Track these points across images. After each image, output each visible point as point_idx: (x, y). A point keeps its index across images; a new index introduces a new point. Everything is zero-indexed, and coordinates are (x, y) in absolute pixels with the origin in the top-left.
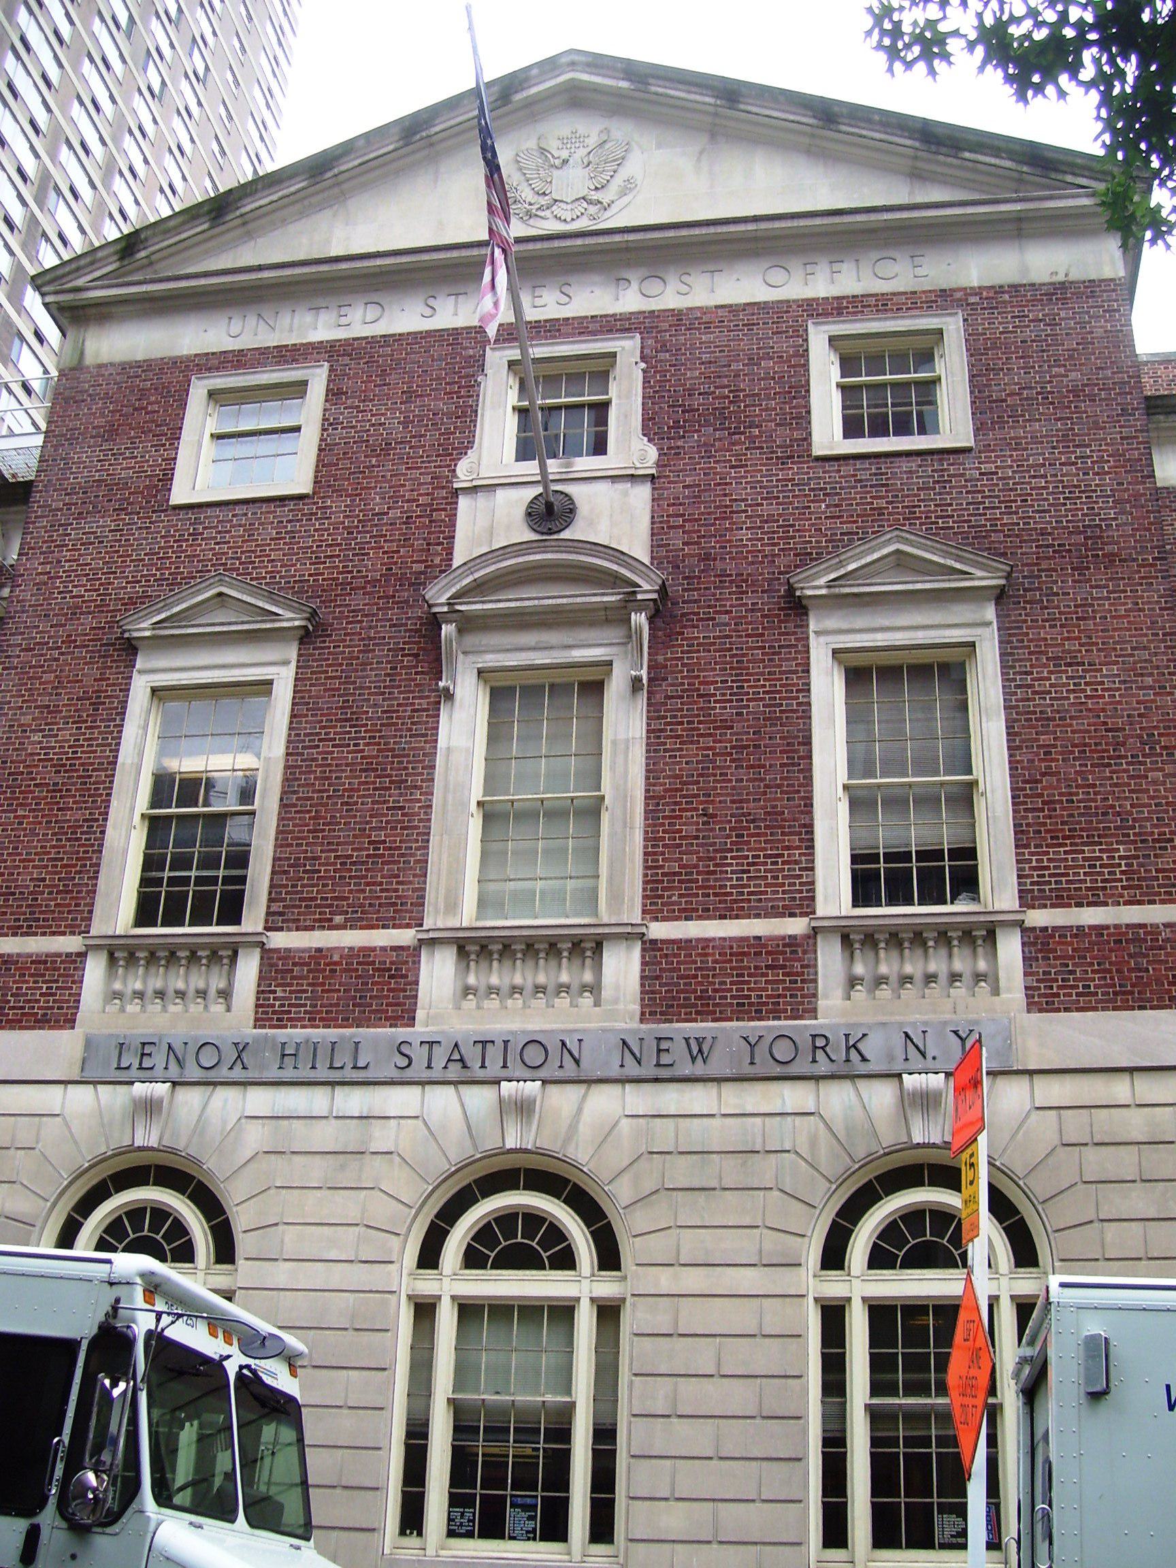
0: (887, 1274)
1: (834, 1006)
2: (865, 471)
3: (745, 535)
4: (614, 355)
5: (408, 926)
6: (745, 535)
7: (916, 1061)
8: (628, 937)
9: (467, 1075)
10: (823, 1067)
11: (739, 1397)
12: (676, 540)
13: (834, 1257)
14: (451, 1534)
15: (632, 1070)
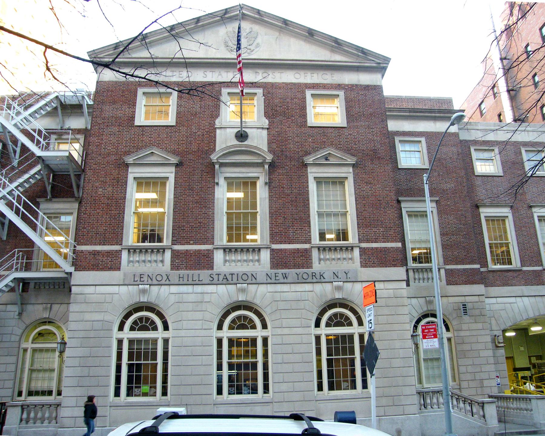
1: (317, 266)
5: (210, 244)
7: (336, 279)
8: (267, 248)
10: (315, 280)
11: (298, 358)
12: (274, 146)
15: (269, 281)
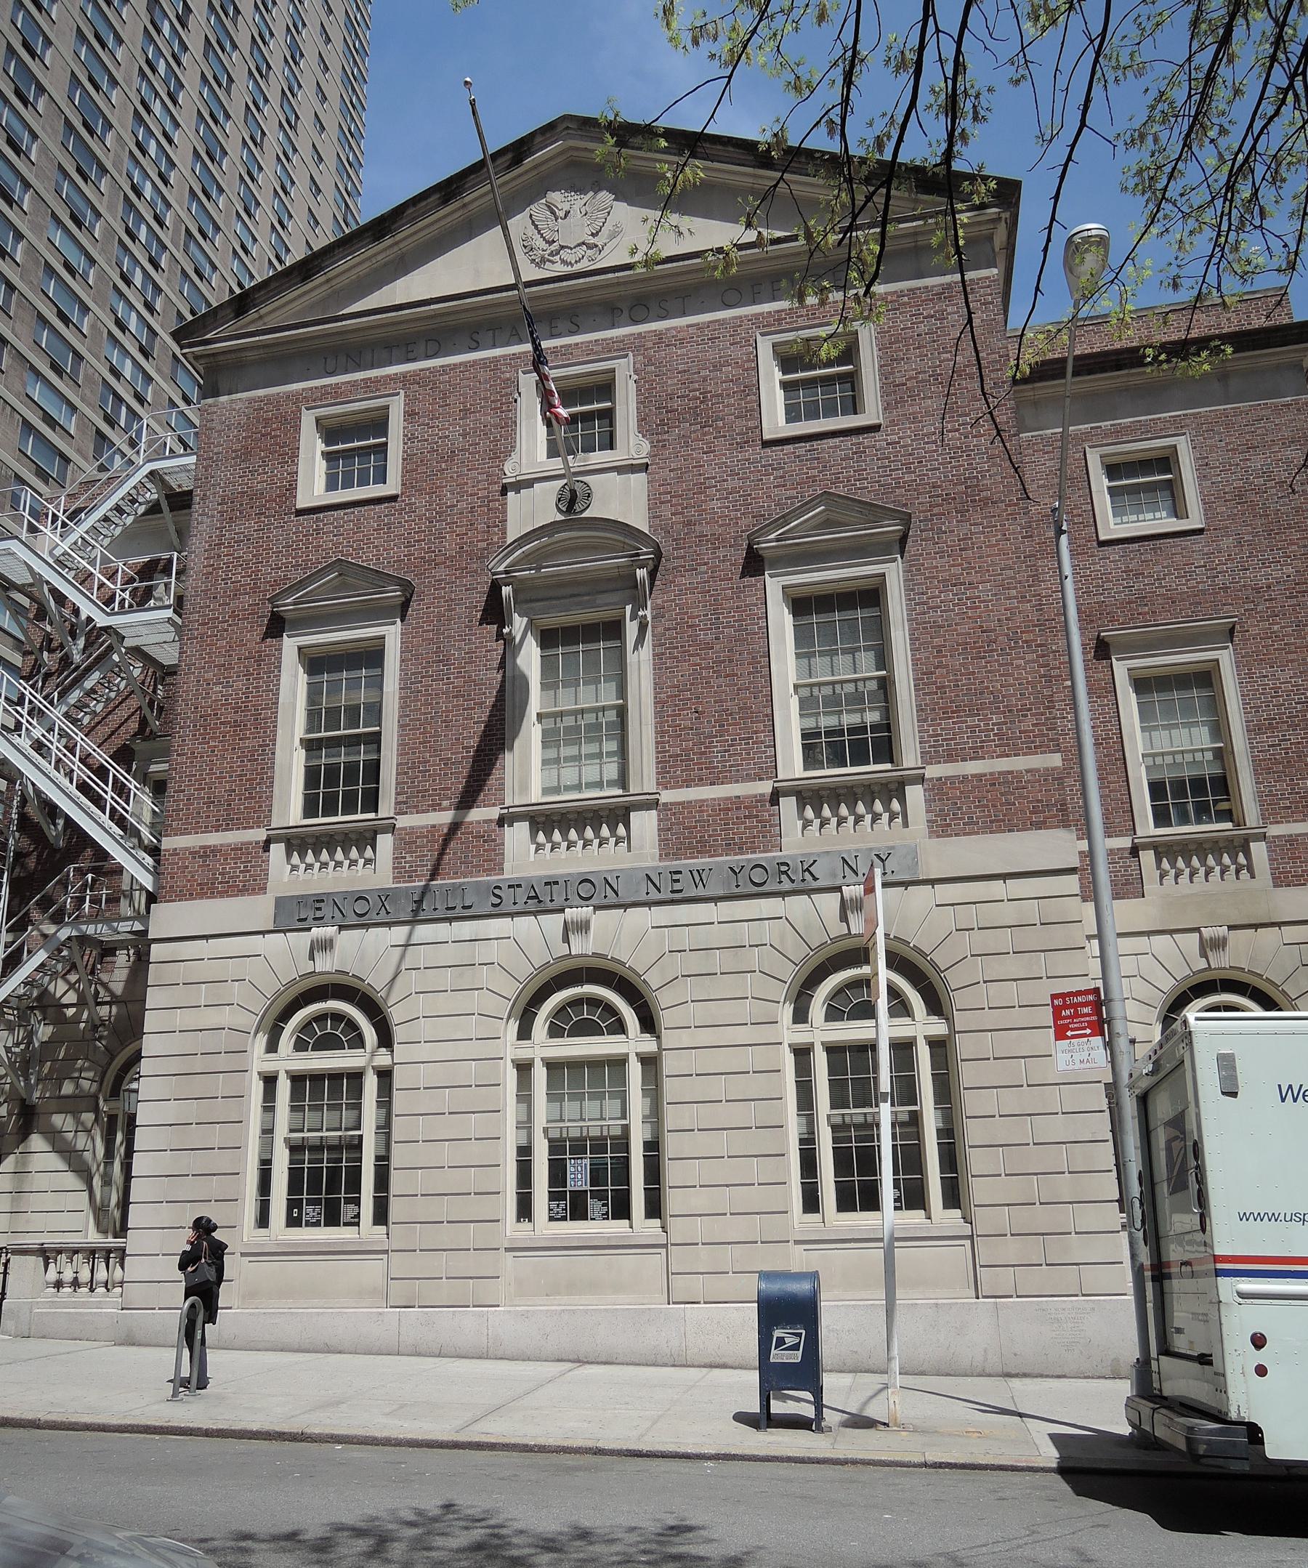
3: (716, 504)
5: (494, 805)
6: (716, 504)
7: (851, 877)
10: (787, 885)
14: (551, 1219)
15: (655, 895)
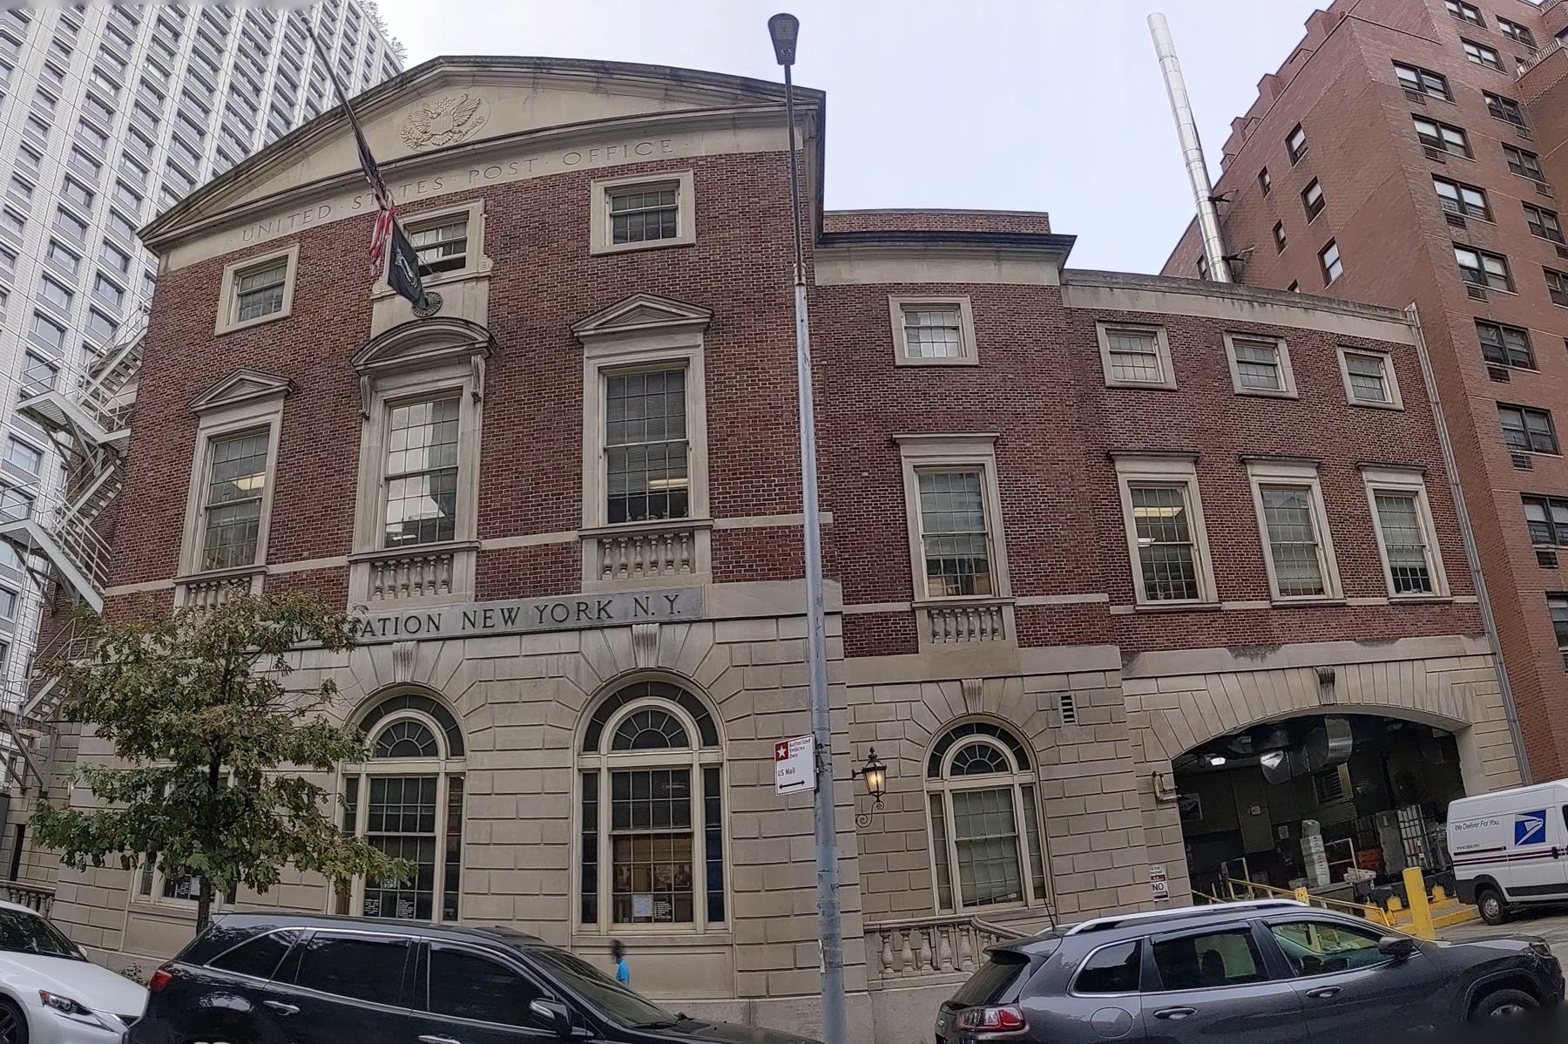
0: (625, 753)
1: (592, 583)
2: (623, 261)
3: (546, 304)
4: (467, 212)
6: (546, 304)
7: (642, 616)
8: (469, 550)
9: (374, 640)
10: (584, 622)
11: (531, 832)
12: (504, 311)
13: (591, 744)
15: (470, 631)
